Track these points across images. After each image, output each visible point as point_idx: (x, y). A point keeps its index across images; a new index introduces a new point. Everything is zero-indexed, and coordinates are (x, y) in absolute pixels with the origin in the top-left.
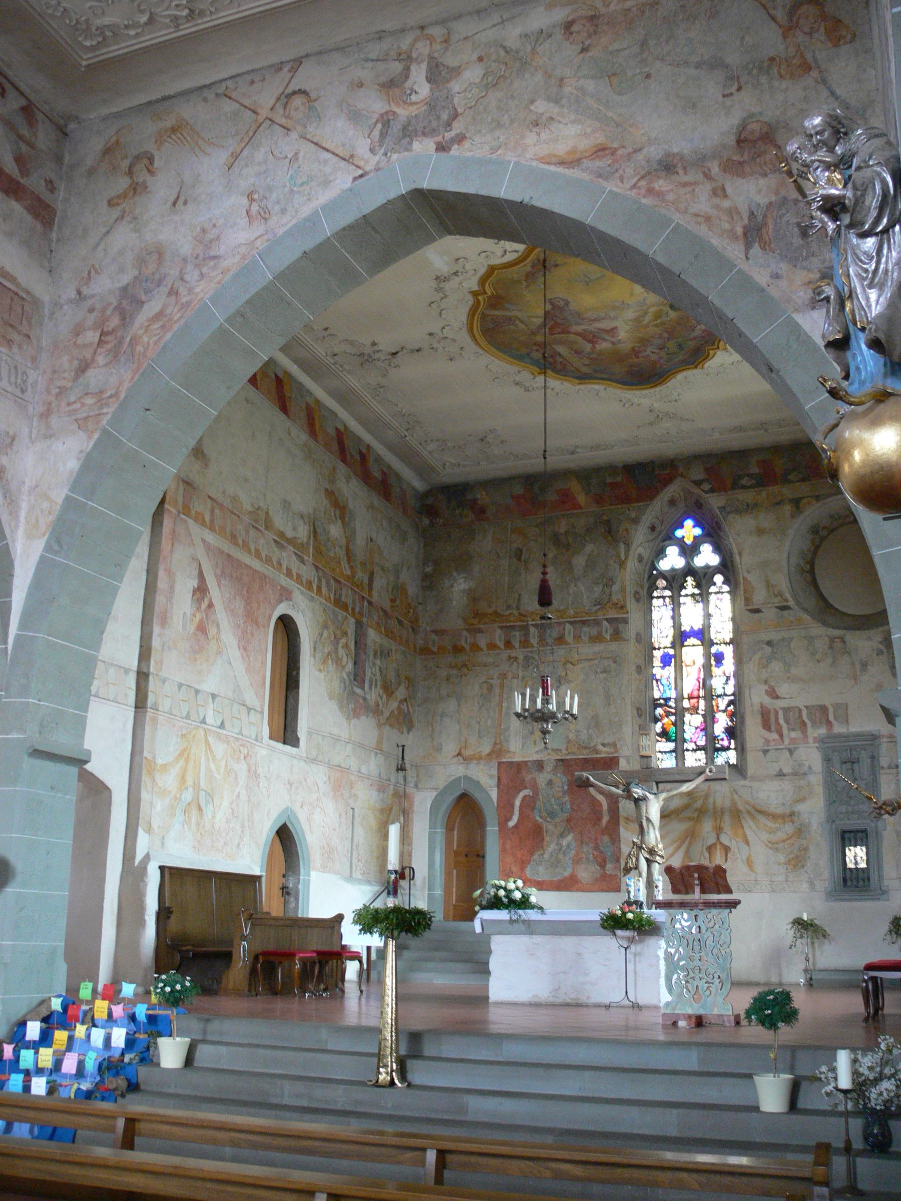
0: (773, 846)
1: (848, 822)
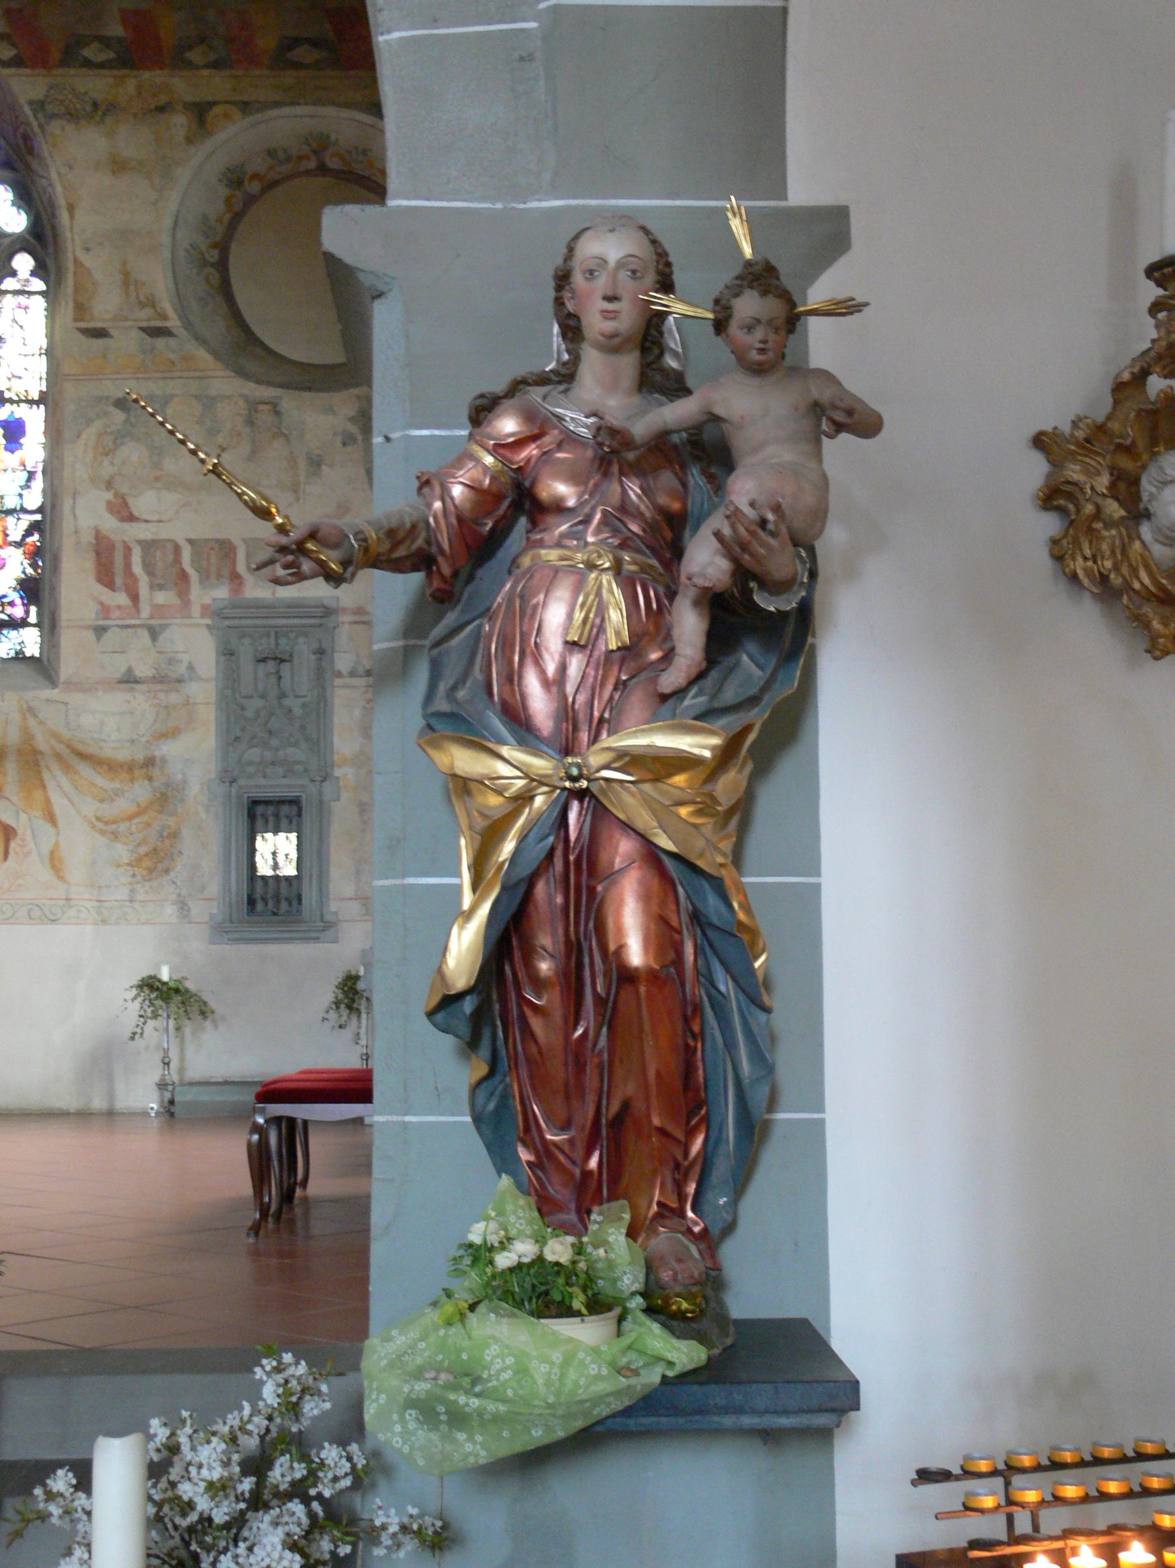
0: (107, 827)
1: (263, 782)
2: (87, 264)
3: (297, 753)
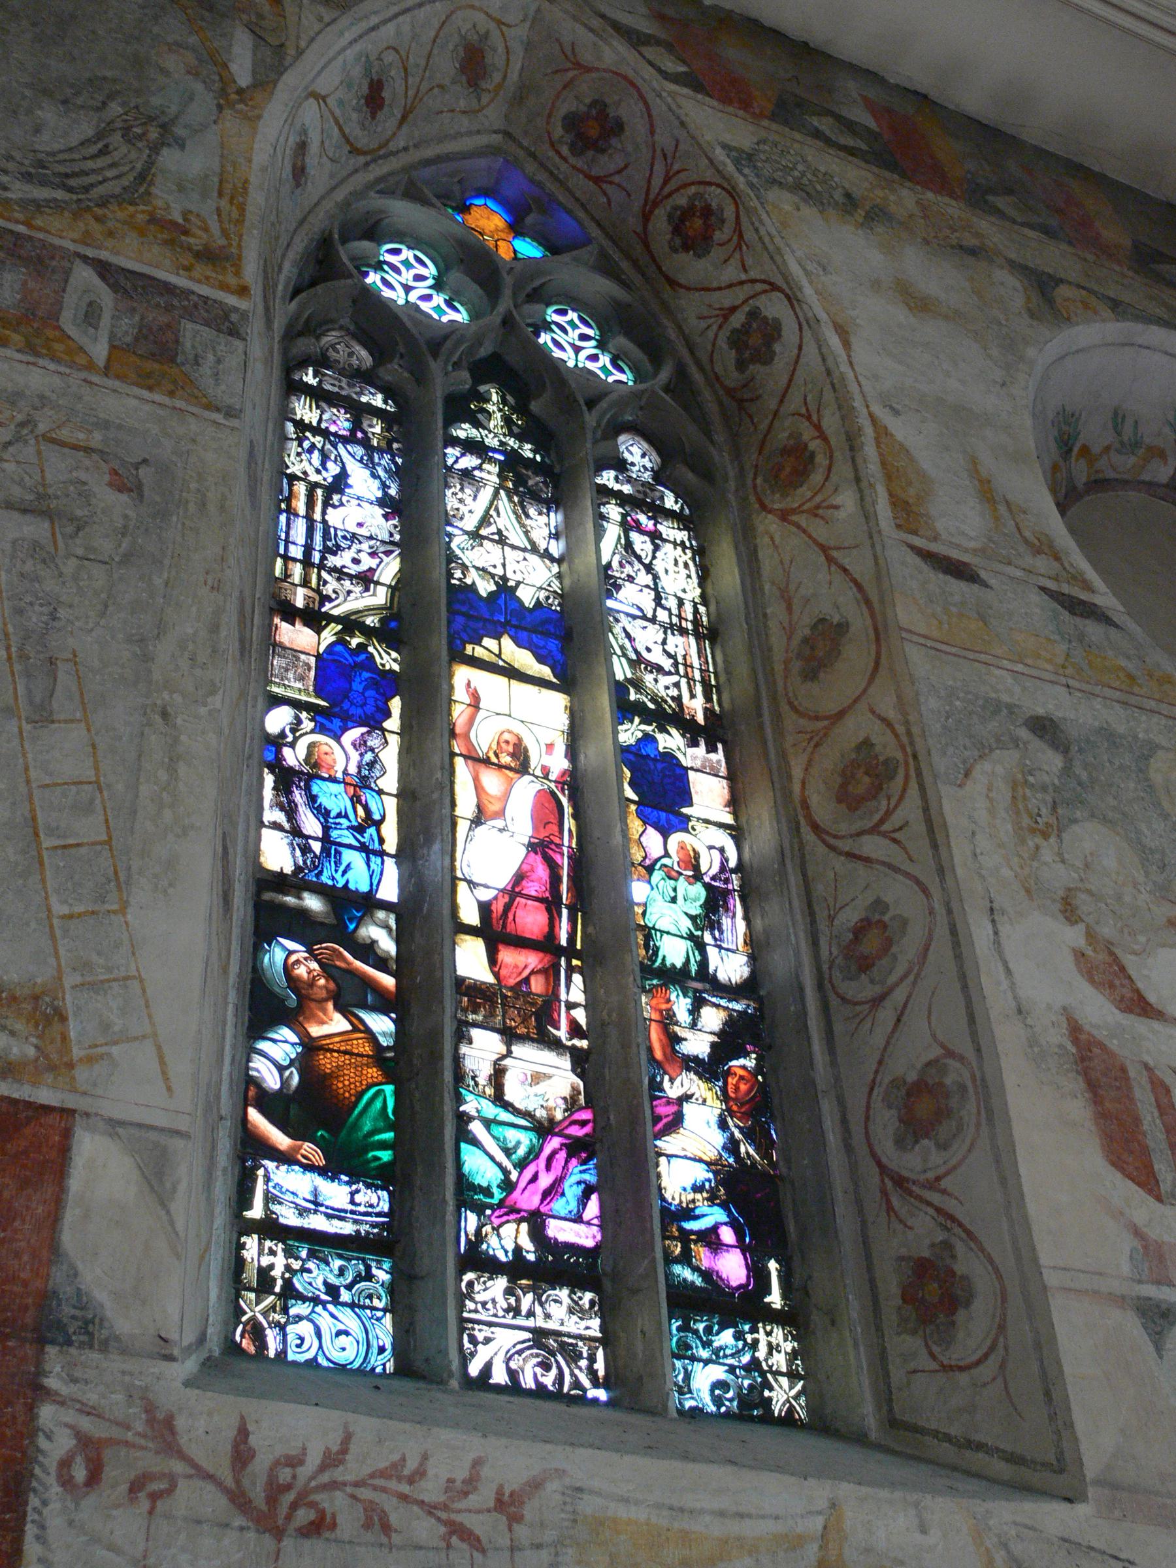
2: (899, 435)
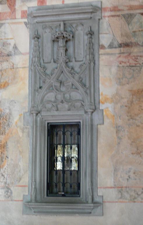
1: (56, 113)
3: (76, 95)
